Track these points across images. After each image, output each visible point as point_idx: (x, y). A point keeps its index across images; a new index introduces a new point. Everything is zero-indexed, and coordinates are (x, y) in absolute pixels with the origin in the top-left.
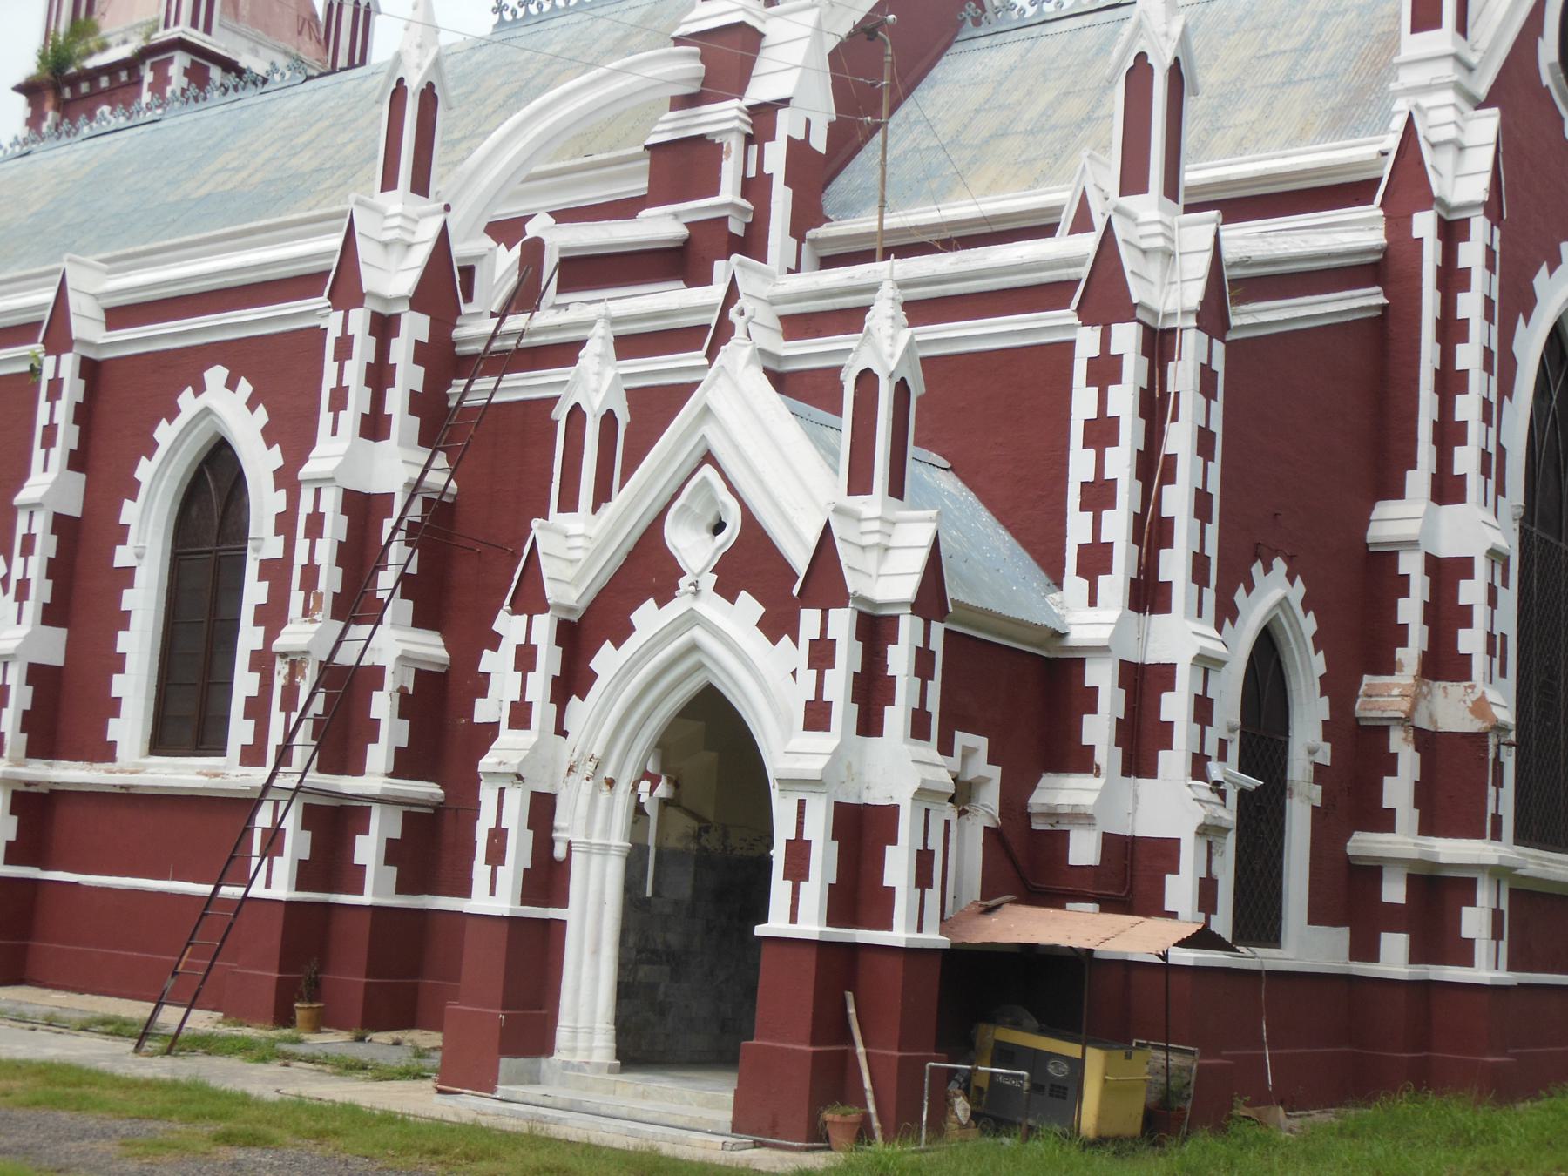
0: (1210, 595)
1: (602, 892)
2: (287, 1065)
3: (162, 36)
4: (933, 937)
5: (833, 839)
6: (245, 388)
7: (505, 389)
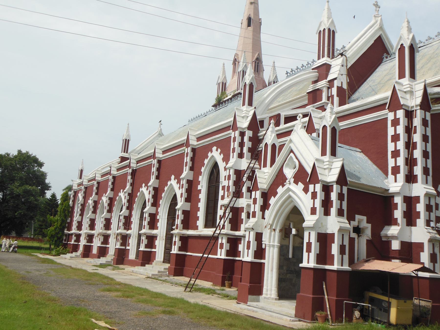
0: (430, 178)
1: (273, 256)
2: (213, 295)
3: (236, 92)
4: (346, 267)
5: (317, 242)
6: (219, 150)
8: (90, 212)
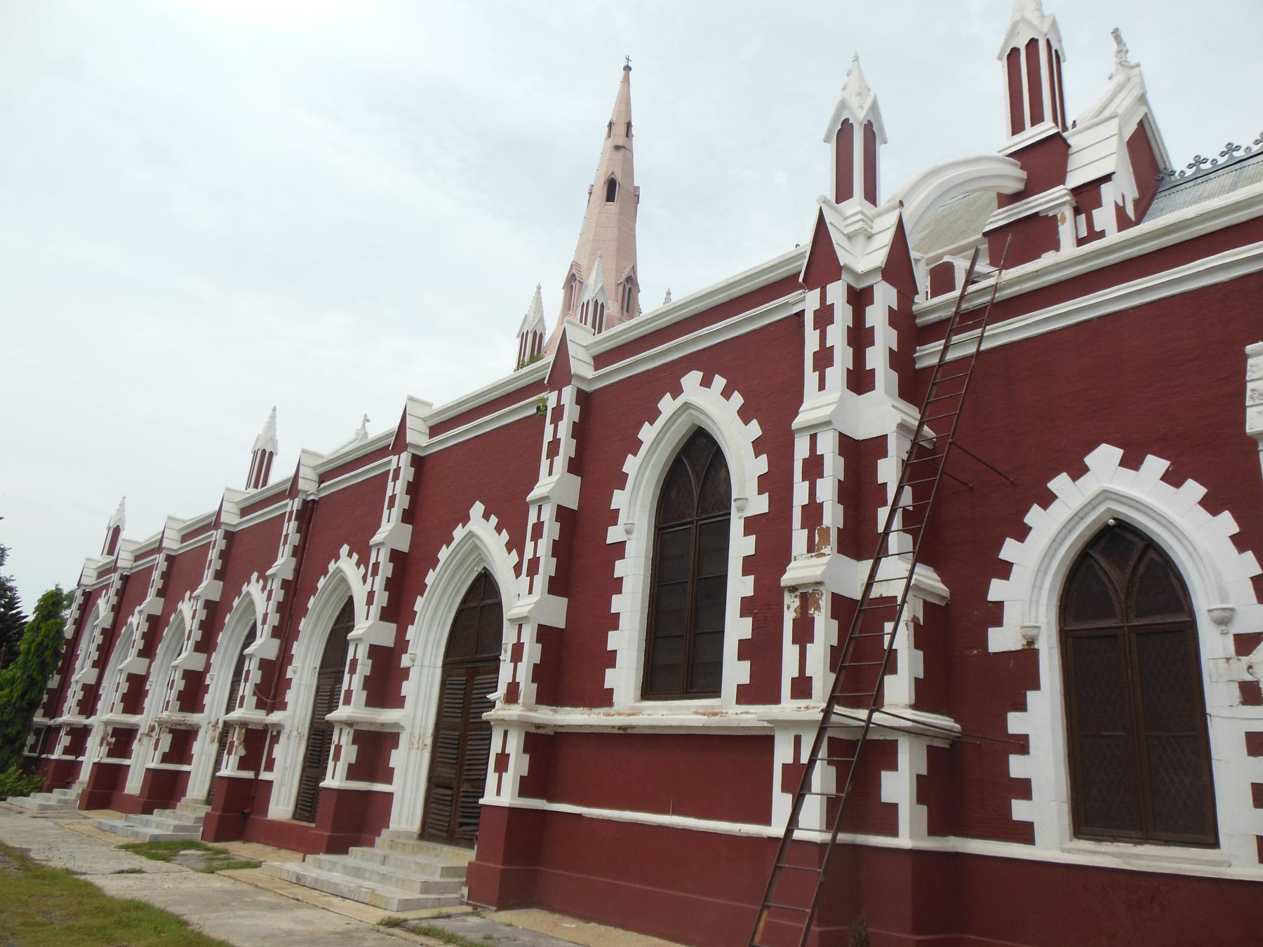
6: (719, 382)
7: (989, 336)
8: (133, 652)
